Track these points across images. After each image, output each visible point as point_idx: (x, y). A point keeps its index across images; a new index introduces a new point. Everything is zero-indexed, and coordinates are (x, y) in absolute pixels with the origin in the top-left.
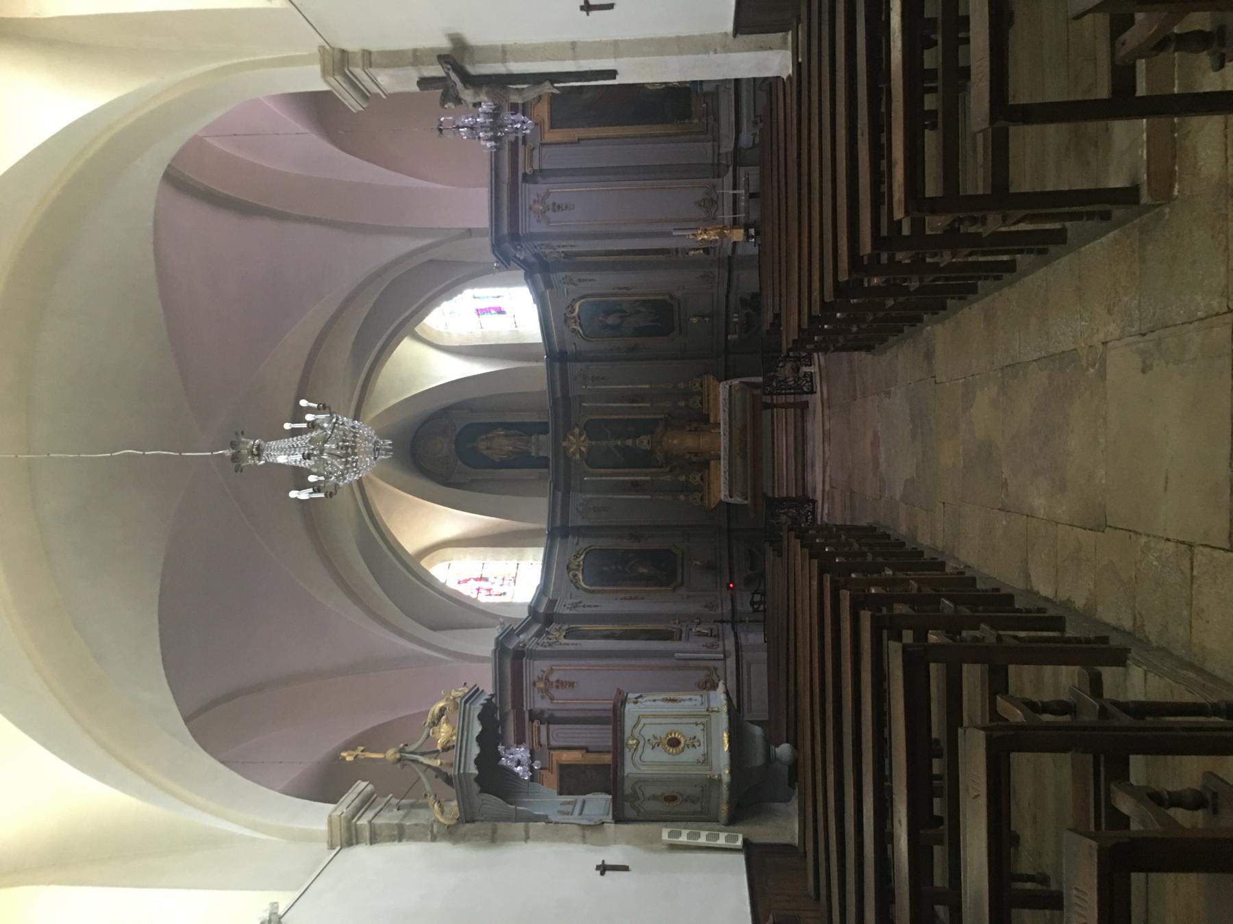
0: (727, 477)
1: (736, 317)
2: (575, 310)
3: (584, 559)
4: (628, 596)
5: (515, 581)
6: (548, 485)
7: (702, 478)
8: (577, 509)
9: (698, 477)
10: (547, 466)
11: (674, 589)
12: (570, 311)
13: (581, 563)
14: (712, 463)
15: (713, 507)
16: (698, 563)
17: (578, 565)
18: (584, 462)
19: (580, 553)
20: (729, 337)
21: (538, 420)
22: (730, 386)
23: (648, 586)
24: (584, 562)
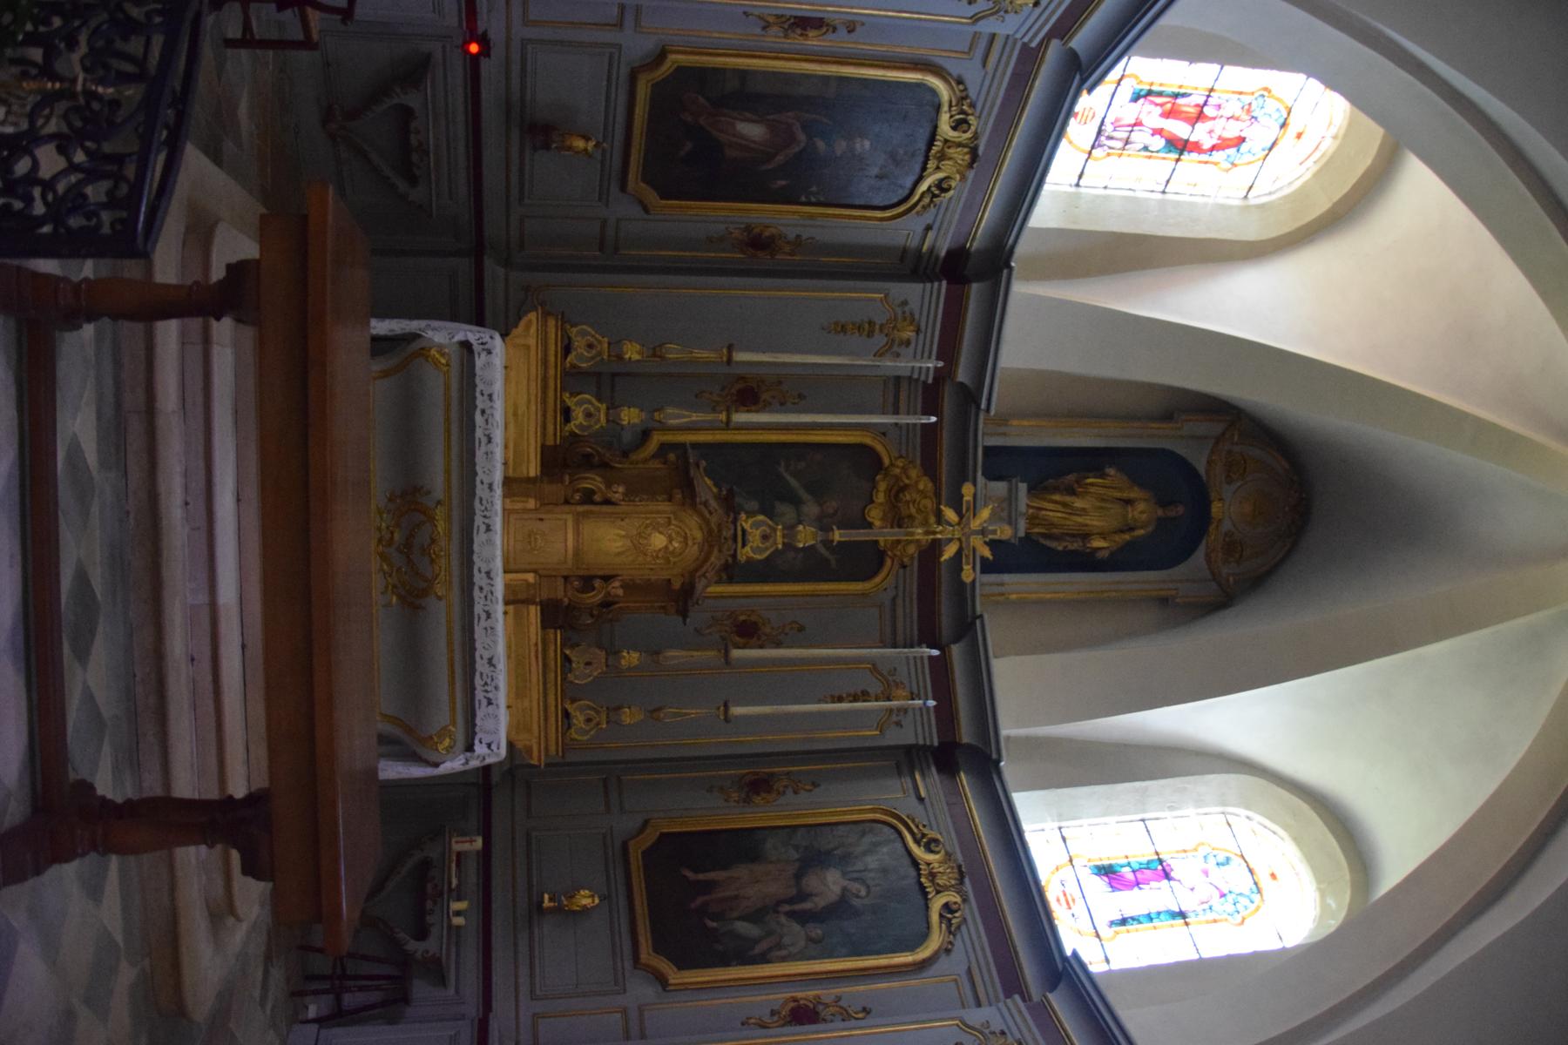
0: (479, 418)
1: (458, 913)
2: (941, 916)
3: (920, 179)
4: (814, 41)
5: (1100, 132)
6: (999, 397)
7: (567, 414)
8: (918, 331)
9: (579, 417)
10: (987, 450)
11: (662, 55)
12: (952, 912)
13: (931, 165)
14: (533, 470)
15: (532, 316)
16: (580, 144)
17: (942, 157)
18: (886, 461)
19: (926, 200)
20: (479, 843)
21: (1006, 578)
22: (470, 748)
23: (743, 74)
24: (924, 168)
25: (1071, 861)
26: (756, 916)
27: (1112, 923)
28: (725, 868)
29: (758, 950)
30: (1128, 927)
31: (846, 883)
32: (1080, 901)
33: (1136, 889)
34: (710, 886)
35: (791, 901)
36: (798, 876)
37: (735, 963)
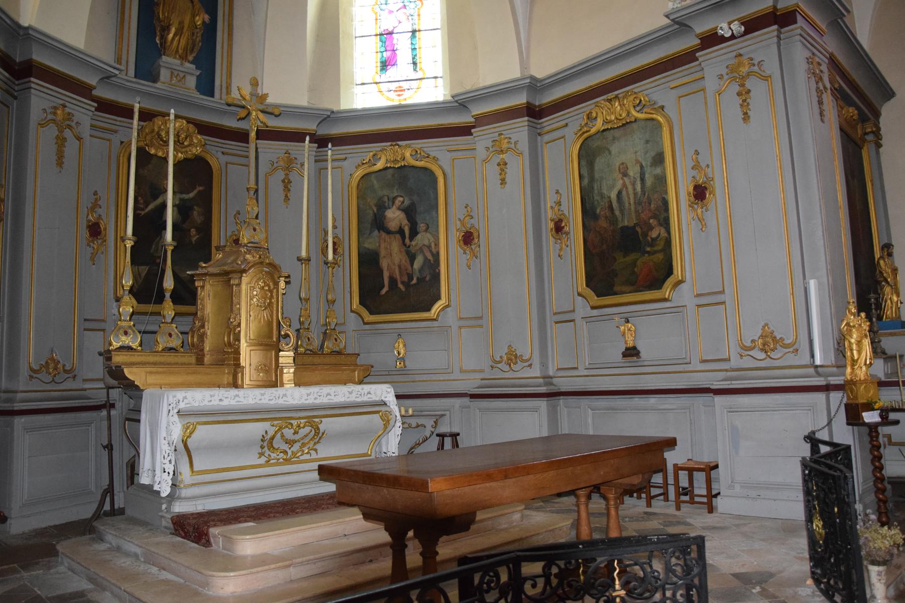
25: (377, 83)
26: (412, 258)
27: (415, 70)
28: (381, 271)
29: (430, 257)
30: (418, 62)
31: (394, 207)
32: (401, 84)
33: (396, 52)
34: (393, 281)
35: (403, 237)
36: (389, 232)
37: (437, 271)
